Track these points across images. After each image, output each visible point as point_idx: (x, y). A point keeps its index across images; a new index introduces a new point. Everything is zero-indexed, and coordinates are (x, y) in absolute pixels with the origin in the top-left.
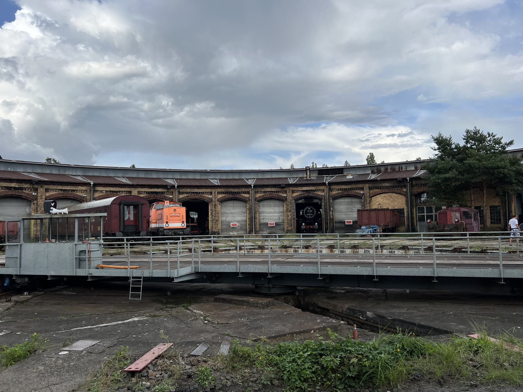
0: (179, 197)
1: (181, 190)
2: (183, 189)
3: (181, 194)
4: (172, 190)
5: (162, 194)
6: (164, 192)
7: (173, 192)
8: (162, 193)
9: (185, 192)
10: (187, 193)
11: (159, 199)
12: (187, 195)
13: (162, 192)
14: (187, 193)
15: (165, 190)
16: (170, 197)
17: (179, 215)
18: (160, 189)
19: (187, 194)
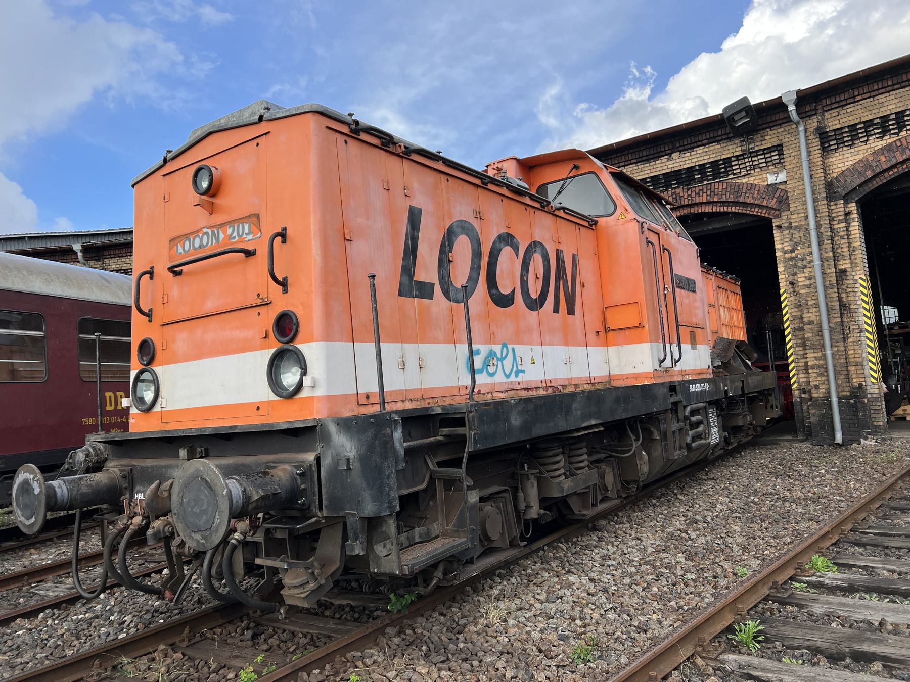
0: (825, 168)
1: (835, 121)
2: (850, 108)
3: (840, 143)
4: (771, 138)
5: (716, 175)
6: (728, 161)
7: (779, 148)
8: (719, 169)
9: (869, 124)
10: (883, 125)
11: (708, 209)
12: (888, 140)
13: (715, 164)
14: (883, 125)
15: (731, 149)
16: (771, 179)
17: (245, 236)
18: (700, 150)
19: (885, 131)
